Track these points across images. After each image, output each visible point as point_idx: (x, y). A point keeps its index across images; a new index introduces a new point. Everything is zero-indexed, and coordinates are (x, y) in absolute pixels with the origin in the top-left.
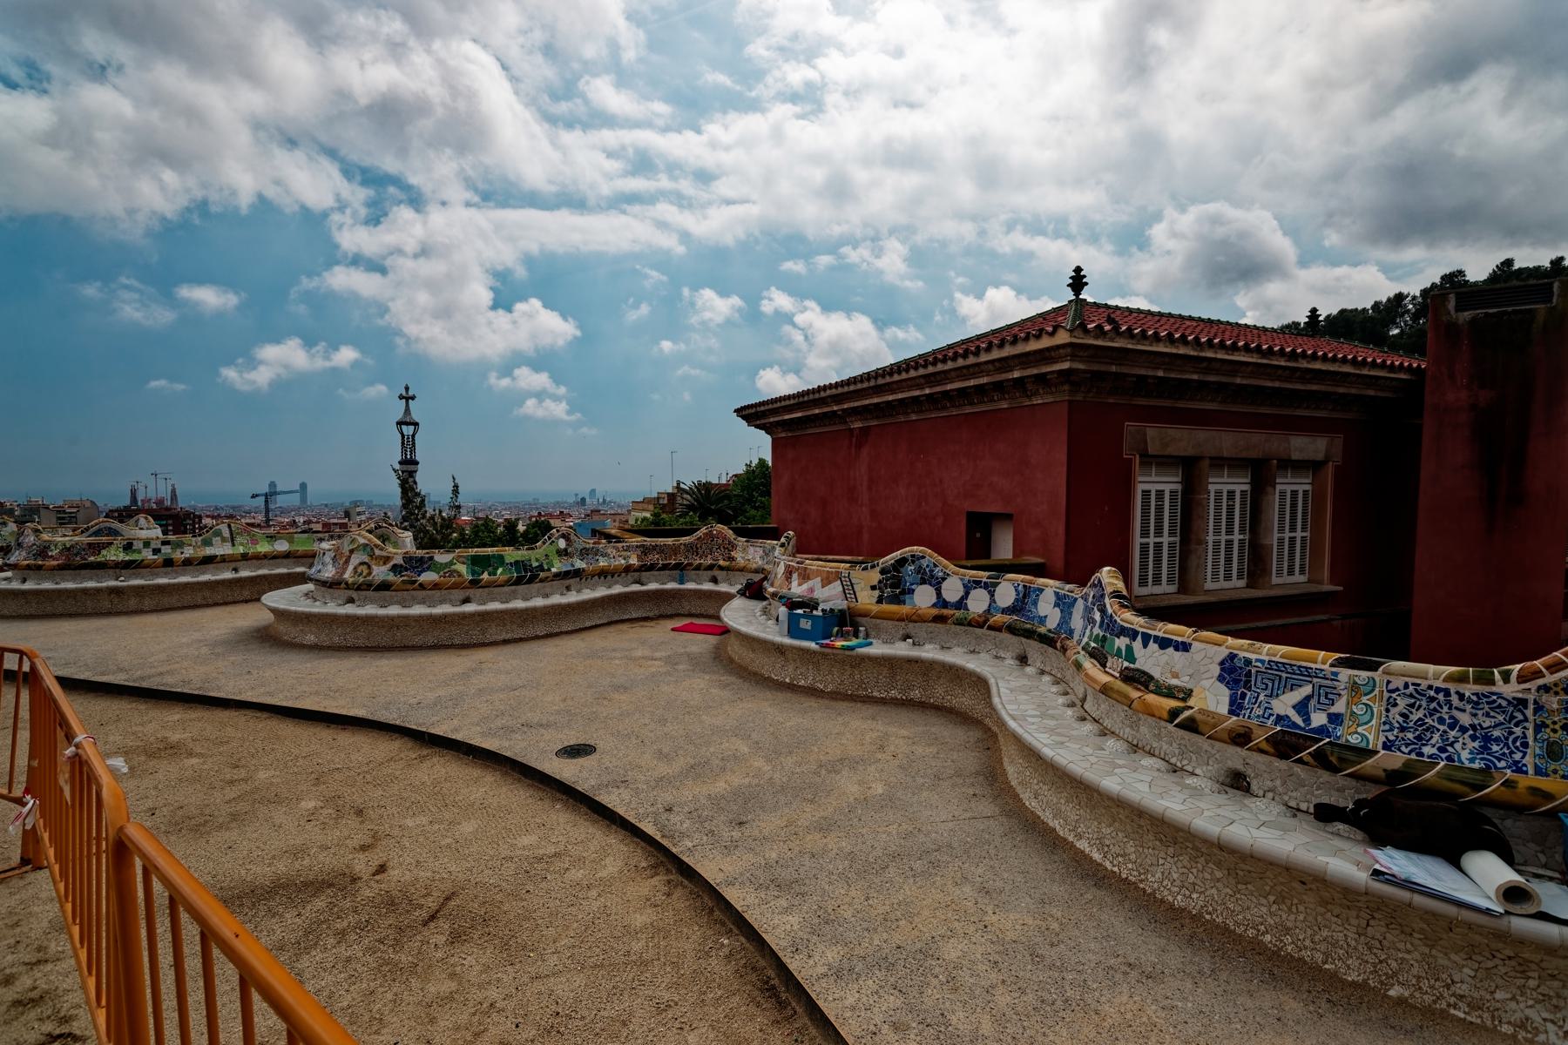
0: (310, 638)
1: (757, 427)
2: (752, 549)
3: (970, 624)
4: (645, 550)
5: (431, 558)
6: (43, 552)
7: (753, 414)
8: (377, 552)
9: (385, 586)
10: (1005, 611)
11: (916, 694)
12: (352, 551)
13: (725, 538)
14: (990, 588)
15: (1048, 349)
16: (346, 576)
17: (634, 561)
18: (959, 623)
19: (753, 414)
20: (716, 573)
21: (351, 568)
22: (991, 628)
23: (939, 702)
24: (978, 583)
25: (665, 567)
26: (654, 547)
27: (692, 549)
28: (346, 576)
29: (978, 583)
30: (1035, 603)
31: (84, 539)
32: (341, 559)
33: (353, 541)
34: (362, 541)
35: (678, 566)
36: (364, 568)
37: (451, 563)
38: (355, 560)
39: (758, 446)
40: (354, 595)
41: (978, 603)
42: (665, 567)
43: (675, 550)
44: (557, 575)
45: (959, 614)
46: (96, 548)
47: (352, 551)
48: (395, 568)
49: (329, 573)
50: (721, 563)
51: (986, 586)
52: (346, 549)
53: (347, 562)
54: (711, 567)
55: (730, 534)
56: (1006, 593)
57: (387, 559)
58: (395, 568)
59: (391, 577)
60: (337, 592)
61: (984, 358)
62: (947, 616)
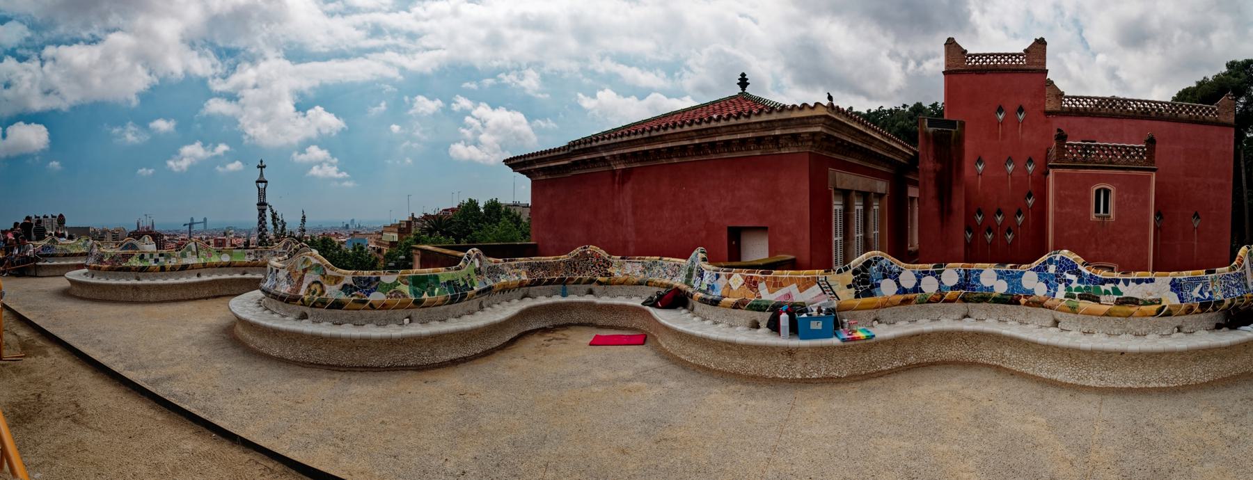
0: (276, 351)
1: (522, 172)
2: (629, 266)
3: (929, 302)
4: (532, 268)
5: (378, 279)
6: (100, 259)
7: (517, 164)
8: (329, 272)
9: (338, 305)
10: (952, 288)
11: (912, 359)
12: (305, 271)
13: (599, 257)
14: (937, 275)
15: (808, 118)
16: (302, 293)
17: (524, 277)
18: (921, 302)
19: (517, 164)
20: (593, 286)
21: (305, 286)
22: (946, 301)
23: (931, 360)
24: (926, 273)
25: (550, 282)
26: (539, 265)
27: (570, 265)
28: (302, 293)
29: (926, 273)
30: (978, 280)
31: (118, 251)
32: (295, 278)
33: (306, 261)
34: (314, 261)
35: (562, 281)
36: (317, 286)
37: (396, 284)
38: (308, 279)
39: (519, 191)
40: (308, 310)
41: (930, 286)
42: (550, 282)
43: (556, 267)
44: (478, 293)
45: (919, 295)
46: (126, 257)
47: (305, 271)
48: (345, 288)
49: (284, 289)
50: (599, 278)
51: (933, 274)
52: (300, 269)
53: (301, 280)
54: (591, 281)
55: (603, 253)
56: (951, 276)
57: (337, 279)
58: (345, 288)
59: (343, 297)
60: (290, 307)
61: (754, 119)
62: (910, 298)
